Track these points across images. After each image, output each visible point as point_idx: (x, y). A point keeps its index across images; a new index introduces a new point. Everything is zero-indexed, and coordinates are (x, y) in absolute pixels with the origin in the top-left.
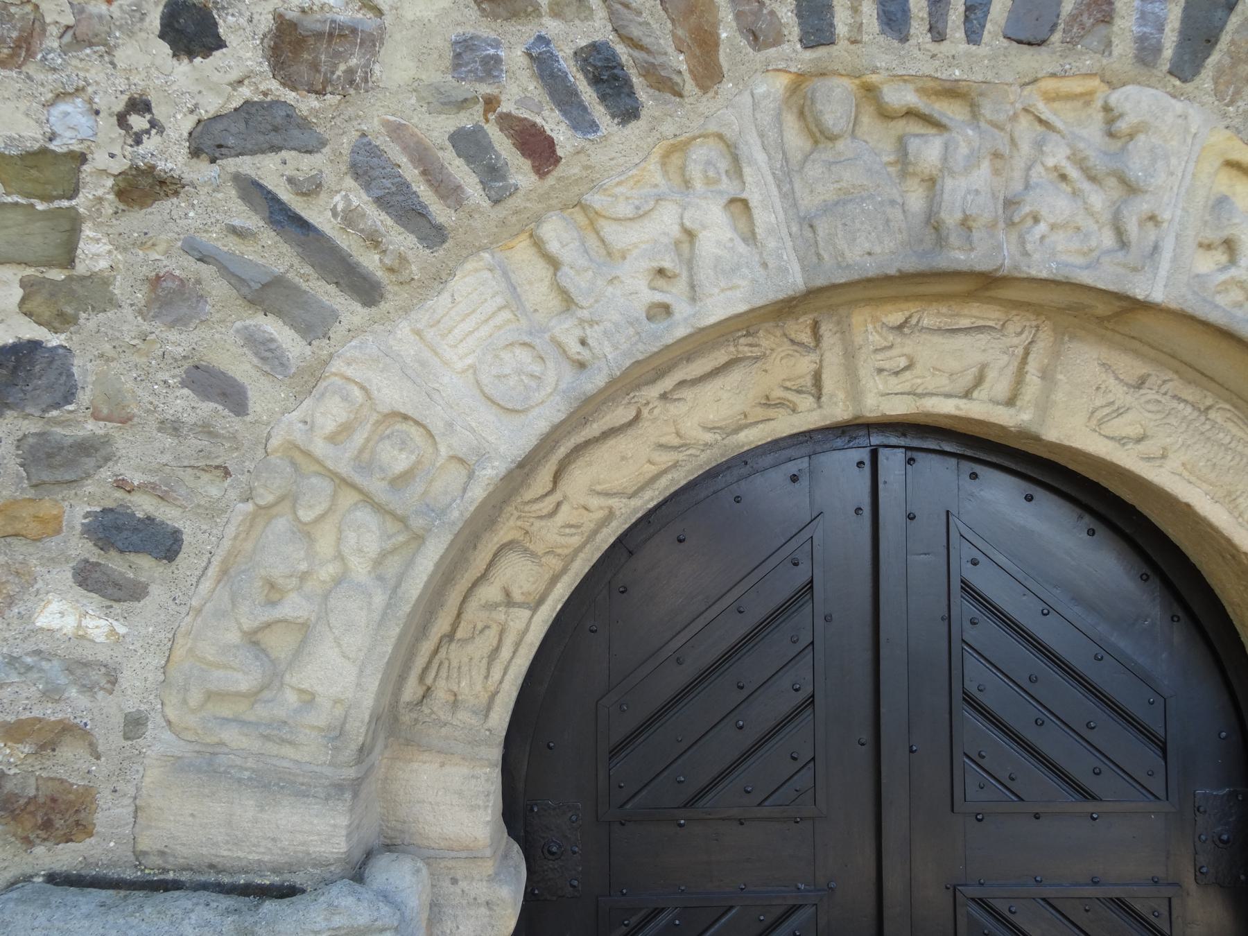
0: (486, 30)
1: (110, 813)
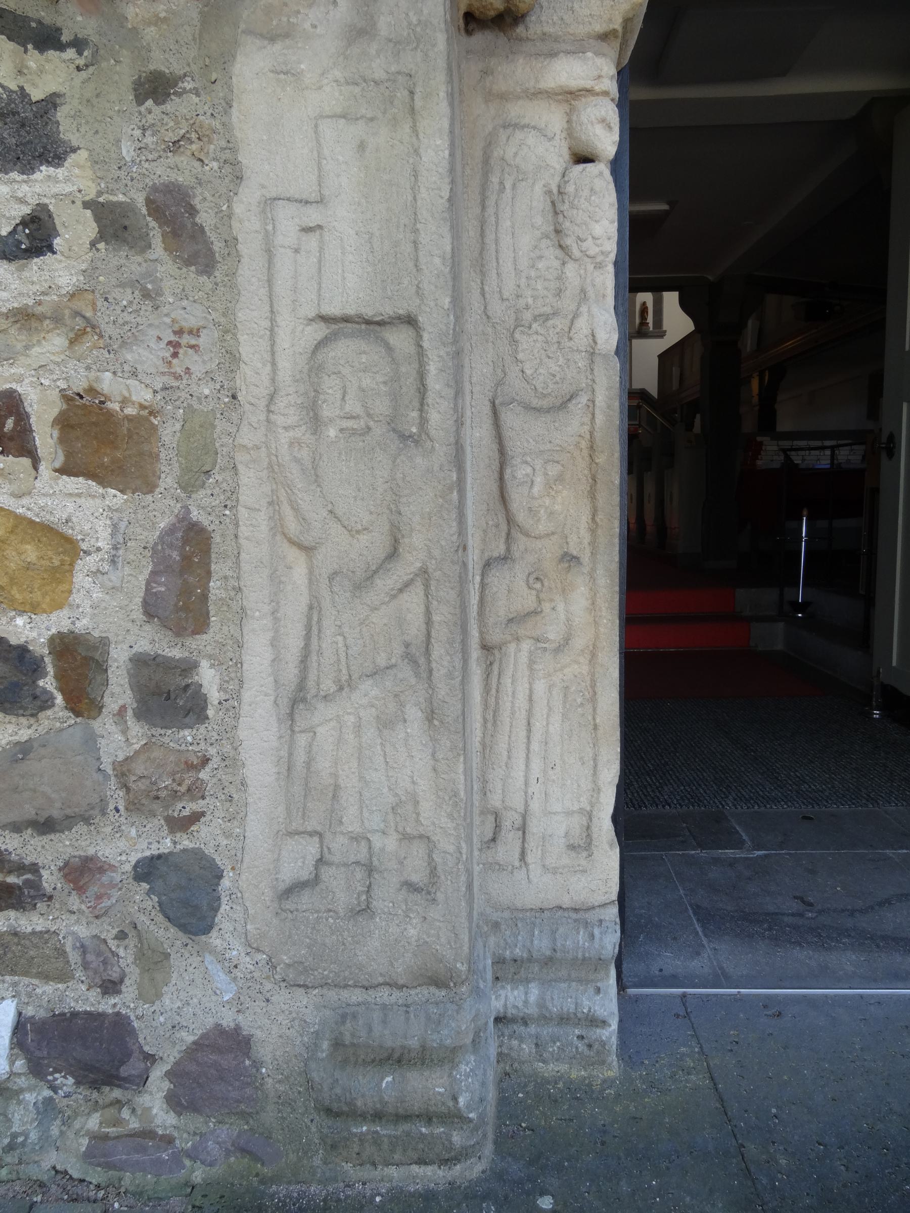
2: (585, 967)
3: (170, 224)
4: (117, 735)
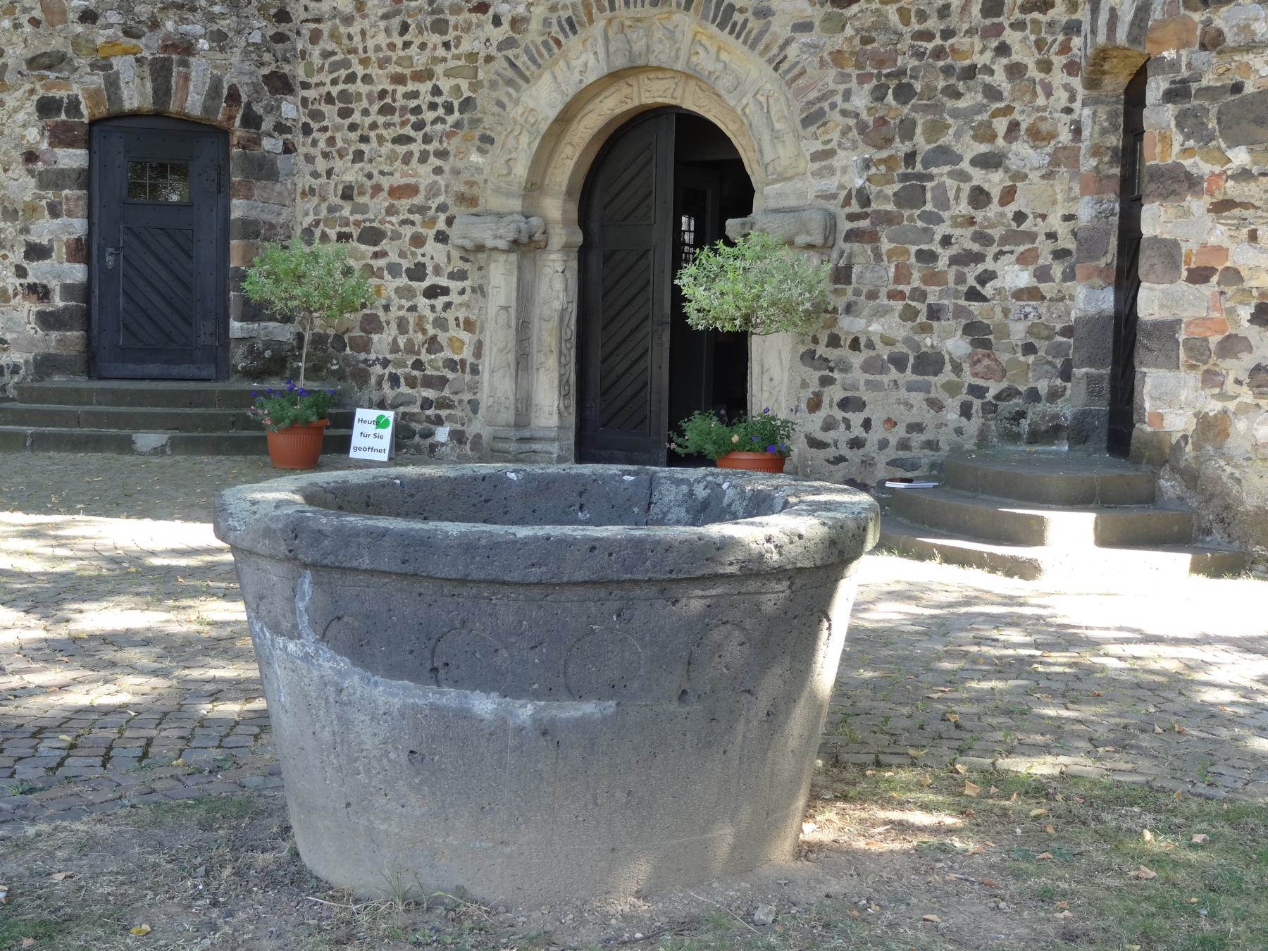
0: (549, 15)
1: (482, 201)
2: (552, 440)
3: (480, 290)
4: (468, 377)
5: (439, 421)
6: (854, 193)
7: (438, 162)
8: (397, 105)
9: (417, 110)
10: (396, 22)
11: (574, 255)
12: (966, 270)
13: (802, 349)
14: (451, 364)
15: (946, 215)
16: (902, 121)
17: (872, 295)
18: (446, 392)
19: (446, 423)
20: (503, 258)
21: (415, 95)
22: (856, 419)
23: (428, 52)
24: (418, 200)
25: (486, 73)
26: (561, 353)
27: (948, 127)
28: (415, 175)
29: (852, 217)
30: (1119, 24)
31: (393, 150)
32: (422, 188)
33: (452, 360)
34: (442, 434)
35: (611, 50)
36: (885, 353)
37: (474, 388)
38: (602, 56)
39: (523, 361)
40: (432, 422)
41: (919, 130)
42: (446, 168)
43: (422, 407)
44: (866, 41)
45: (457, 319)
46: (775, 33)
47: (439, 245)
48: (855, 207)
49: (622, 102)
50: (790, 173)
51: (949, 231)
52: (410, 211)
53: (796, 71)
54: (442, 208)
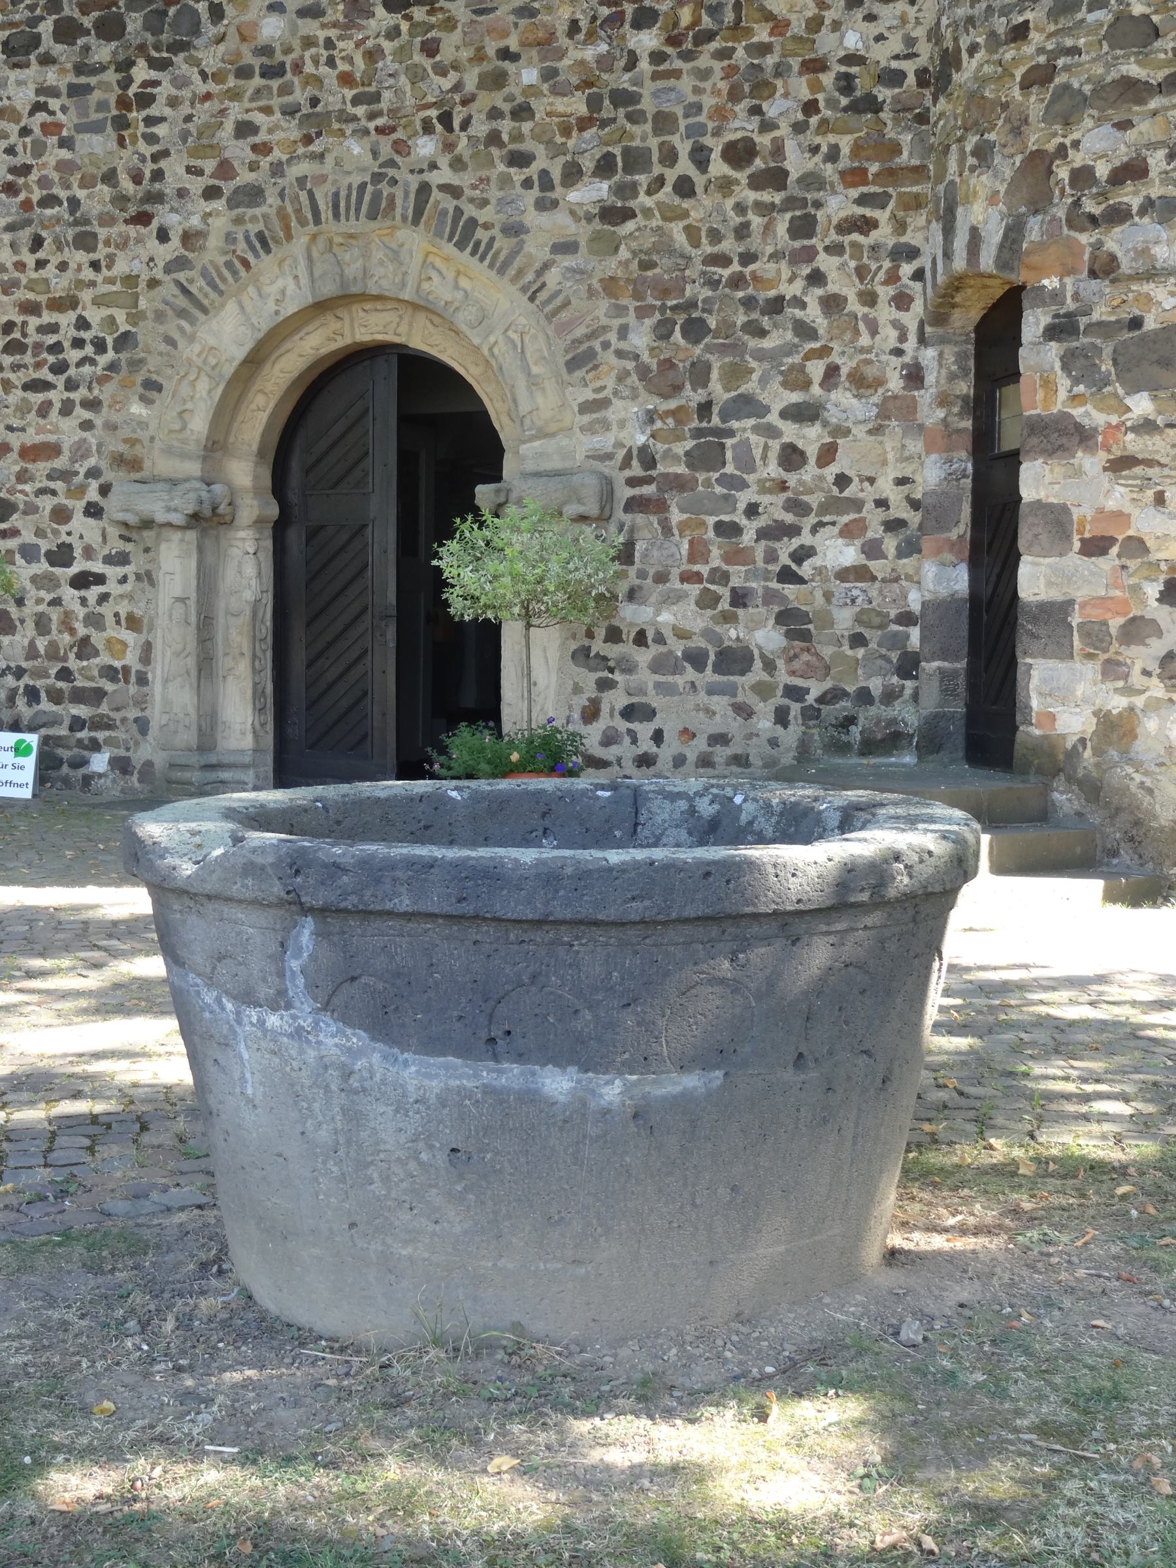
0: (234, 229)
1: (147, 464)
2: (246, 767)
3: (147, 578)
4: (133, 689)
5: (95, 746)
6: (635, 453)
7: (87, 415)
8: (29, 341)
9: (56, 348)
10: (25, 235)
11: (268, 532)
12: (777, 545)
13: (574, 646)
14: (110, 673)
15: (750, 478)
16: (693, 364)
17: (661, 578)
18: (104, 709)
19: (105, 748)
20: (177, 536)
21: (53, 328)
22: (645, 730)
23: (70, 274)
24: (60, 463)
25: (149, 301)
26: (254, 657)
27: (751, 371)
28: (56, 430)
29: (632, 482)
30: (984, 247)
31: (24, 399)
32: (65, 448)
33: (111, 667)
34: (99, 762)
35: (317, 273)
36: (678, 648)
37: (141, 702)
38: (304, 280)
39: (205, 666)
40: (86, 748)
41: (715, 375)
42: (98, 422)
43: (71, 729)
44: (646, 265)
45: (117, 615)
46: (530, 255)
47: (91, 521)
48: (636, 470)
49: (329, 339)
50: (553, 427)
51: (755, 498)
52: (50, 477)
53: (558, 302)
54: (93, 473)
